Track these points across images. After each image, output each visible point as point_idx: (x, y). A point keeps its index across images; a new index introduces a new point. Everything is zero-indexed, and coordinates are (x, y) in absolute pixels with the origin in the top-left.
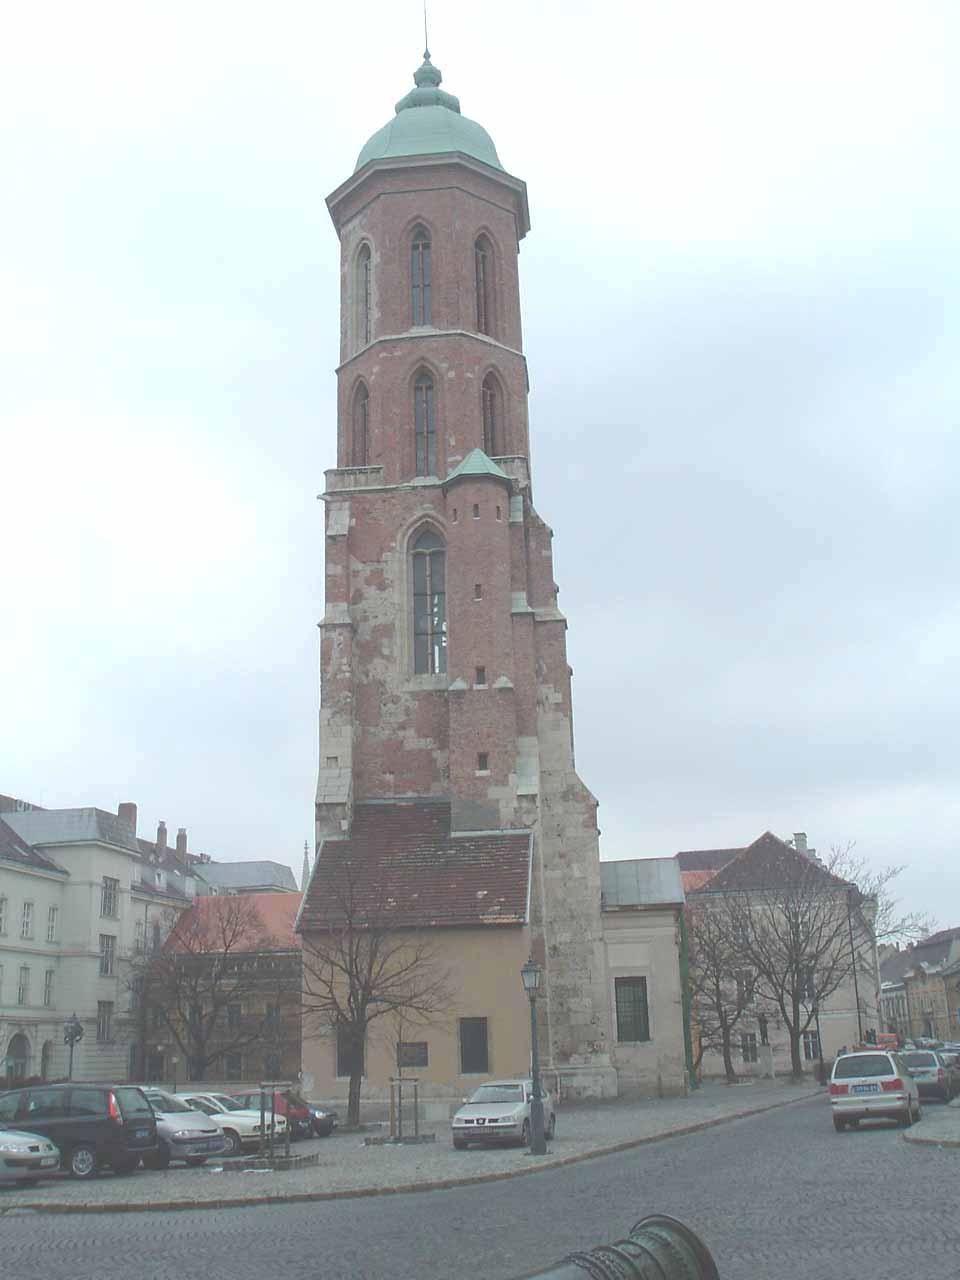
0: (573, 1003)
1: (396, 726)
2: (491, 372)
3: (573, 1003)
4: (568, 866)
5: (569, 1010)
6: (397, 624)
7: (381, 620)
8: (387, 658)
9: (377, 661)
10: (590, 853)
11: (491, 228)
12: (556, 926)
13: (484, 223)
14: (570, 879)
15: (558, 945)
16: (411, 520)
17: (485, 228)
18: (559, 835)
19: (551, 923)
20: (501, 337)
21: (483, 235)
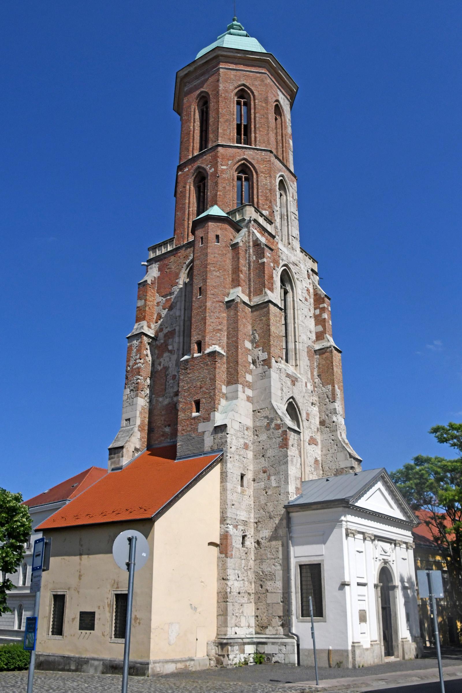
0: (269, 585)
1: (172, 395)
2: (244, 164)
3: (269, 585)
4: (269, 479)
5: (267, 591)
6: (177, 329)
7: (169, 329)
8: (170, 352)
9: (166, 355)
10: (283, 467)
11: (247, 84)
12: (260, 526)
13: (240, 83)
14: (269, 488)
15: (260, 540)
16: (187, 263)
17: (244, 85)
18: (263, 456)
19: (256, 523)
20: (253, 142)
21: (242, 90)
